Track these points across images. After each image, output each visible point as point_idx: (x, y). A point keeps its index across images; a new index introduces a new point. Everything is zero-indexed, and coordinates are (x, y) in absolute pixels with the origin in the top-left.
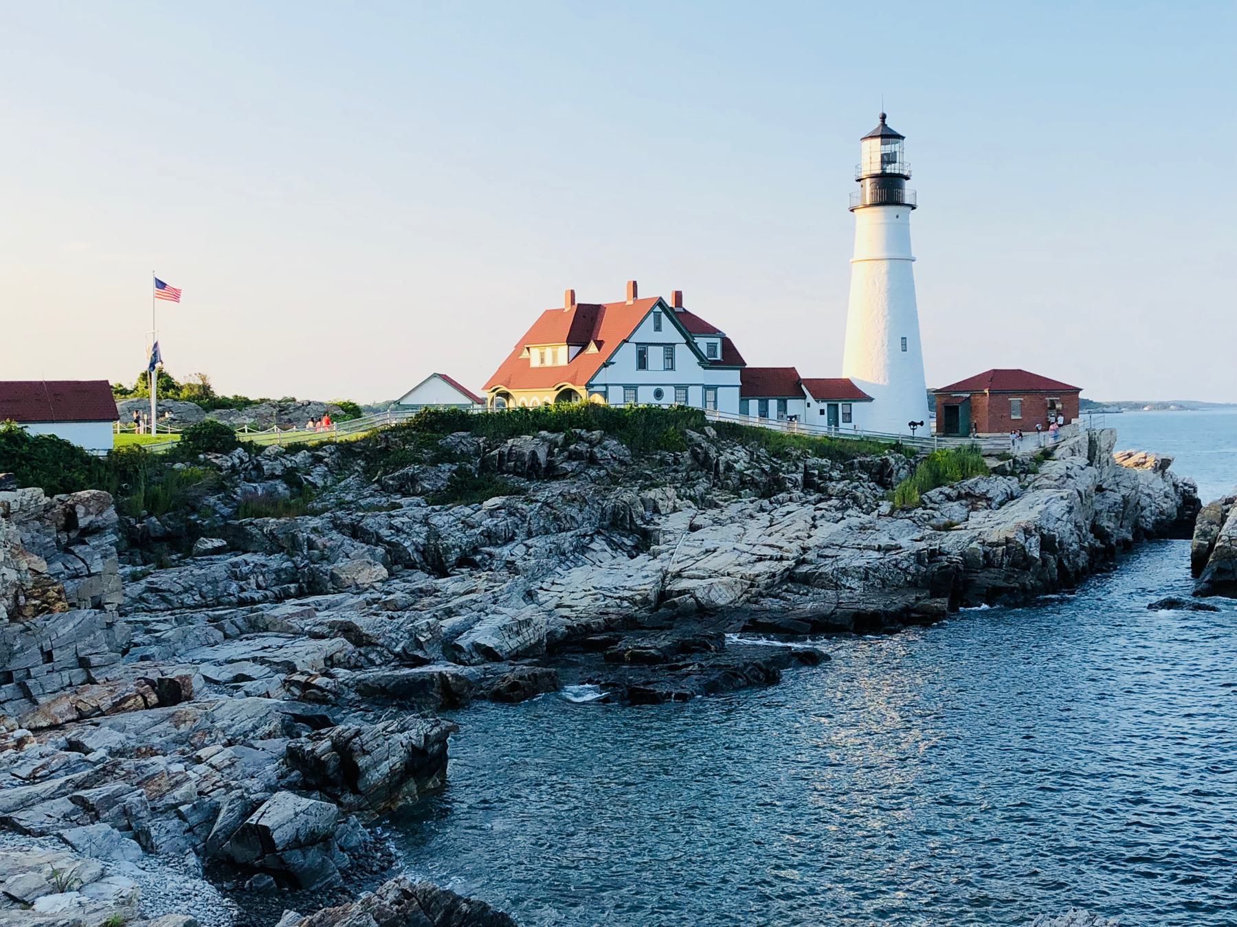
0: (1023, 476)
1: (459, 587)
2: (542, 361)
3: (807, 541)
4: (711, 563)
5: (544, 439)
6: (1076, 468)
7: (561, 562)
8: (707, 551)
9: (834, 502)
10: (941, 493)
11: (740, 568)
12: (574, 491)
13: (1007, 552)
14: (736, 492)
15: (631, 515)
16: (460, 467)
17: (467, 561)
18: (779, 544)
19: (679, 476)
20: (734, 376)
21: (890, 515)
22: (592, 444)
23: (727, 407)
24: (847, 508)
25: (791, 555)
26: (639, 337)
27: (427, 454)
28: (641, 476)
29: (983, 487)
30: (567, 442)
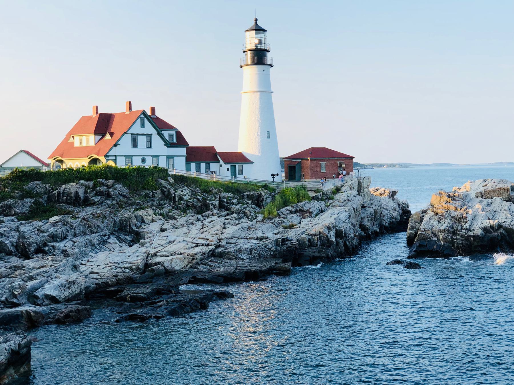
0: (327, 201)
1: (37, 264)
2: (81, 143)
3: (221, 236)
4: (173, 248)
5: (82, 185)
6: (352, 196)
7: (92, 249)
8: (170, 242)
9: (235, 215)
10: (287, 210)
11: (187, 250)
12: (99, 212)
13: (319, 239)
14: (184, 211)
15: (130, 224)
16: (36, 200)
17: (41, 250)
18: (207, 237)
19: (155, 203)
20: (183, 151)
21: (263, 221)
23: (179, 167)
24: (241, 218)
25: (213, 243)
26: (133, 130)
27: (17, 193)
28: (134, 203)
29: (307, 207)
30: (95, 186)
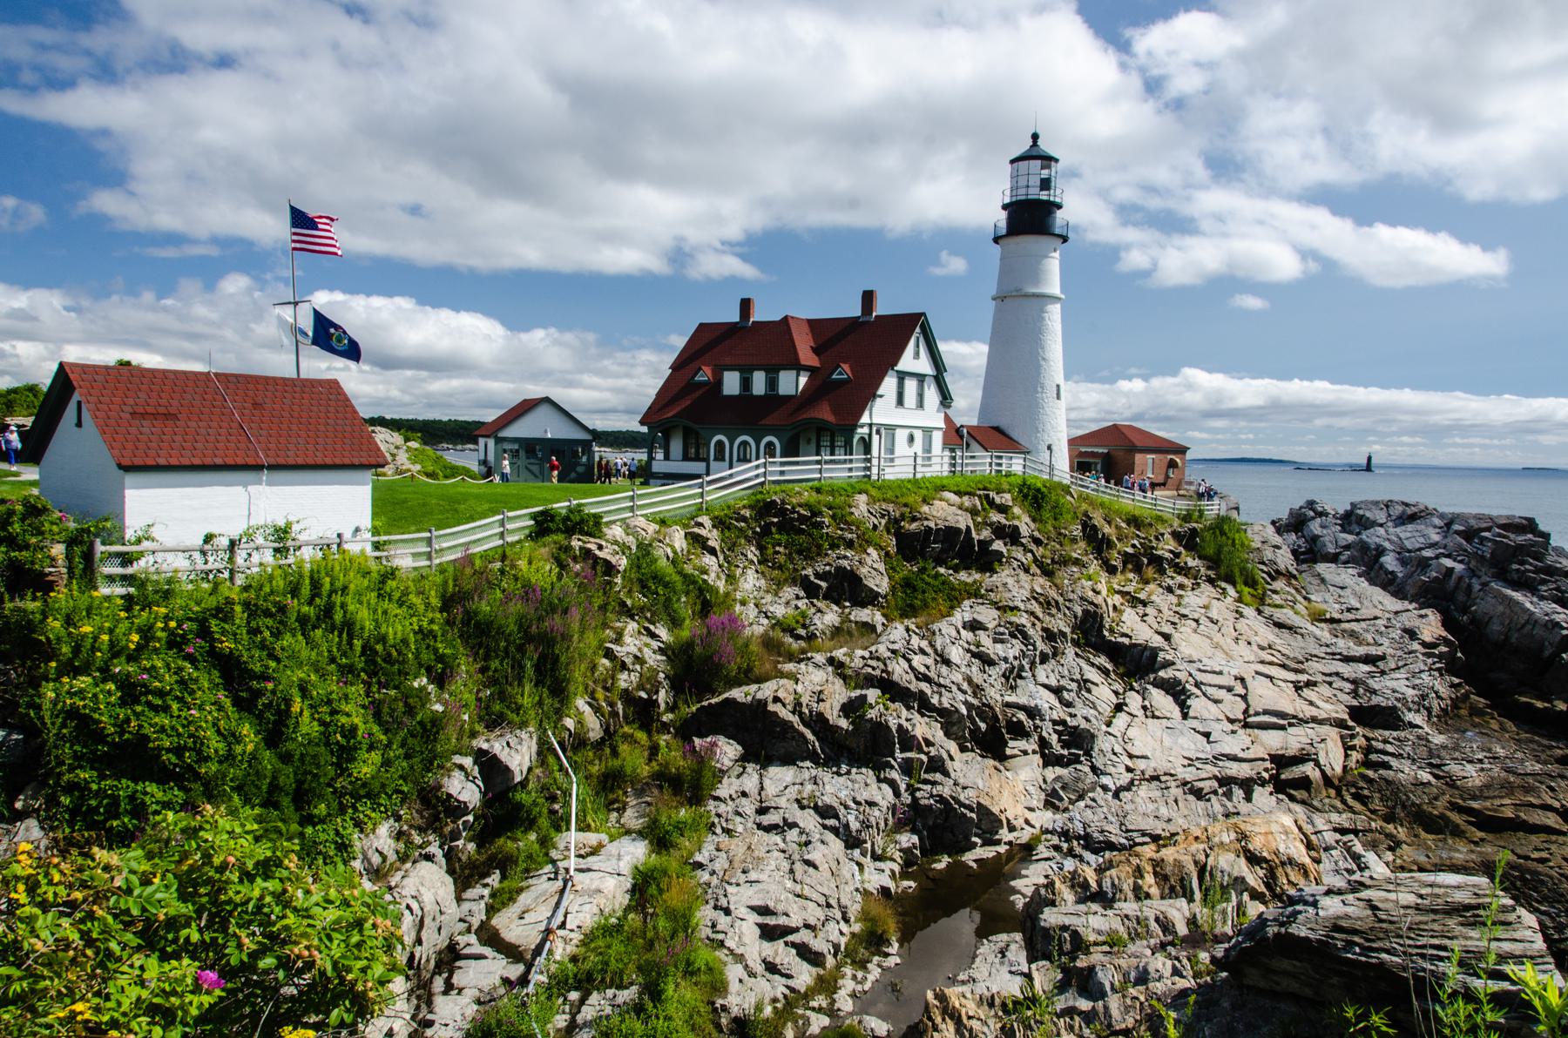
22: (1003, 509)
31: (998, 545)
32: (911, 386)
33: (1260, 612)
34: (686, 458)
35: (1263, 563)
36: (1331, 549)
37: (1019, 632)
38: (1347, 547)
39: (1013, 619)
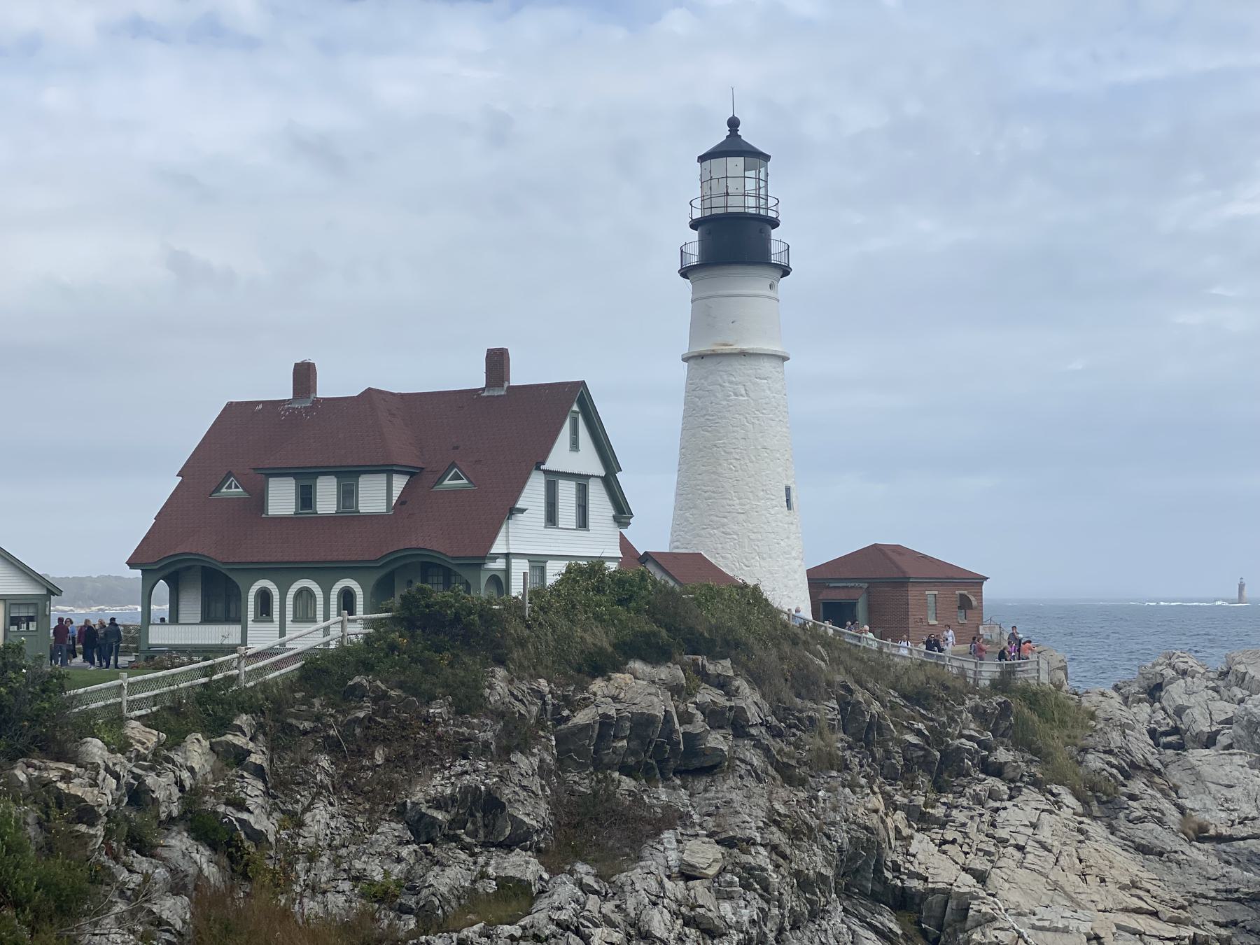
31: (717, 741)
32: (567, 492)
33: (1113, 830)
34: (207, 619)
35: (1110, 752)
36: (1205, 727)
37: (752, 878)
38: (1228, 722)
39: (745, 858)
